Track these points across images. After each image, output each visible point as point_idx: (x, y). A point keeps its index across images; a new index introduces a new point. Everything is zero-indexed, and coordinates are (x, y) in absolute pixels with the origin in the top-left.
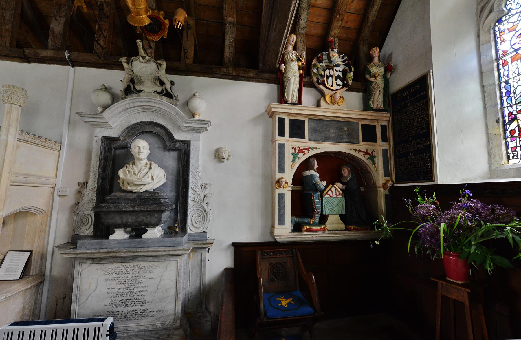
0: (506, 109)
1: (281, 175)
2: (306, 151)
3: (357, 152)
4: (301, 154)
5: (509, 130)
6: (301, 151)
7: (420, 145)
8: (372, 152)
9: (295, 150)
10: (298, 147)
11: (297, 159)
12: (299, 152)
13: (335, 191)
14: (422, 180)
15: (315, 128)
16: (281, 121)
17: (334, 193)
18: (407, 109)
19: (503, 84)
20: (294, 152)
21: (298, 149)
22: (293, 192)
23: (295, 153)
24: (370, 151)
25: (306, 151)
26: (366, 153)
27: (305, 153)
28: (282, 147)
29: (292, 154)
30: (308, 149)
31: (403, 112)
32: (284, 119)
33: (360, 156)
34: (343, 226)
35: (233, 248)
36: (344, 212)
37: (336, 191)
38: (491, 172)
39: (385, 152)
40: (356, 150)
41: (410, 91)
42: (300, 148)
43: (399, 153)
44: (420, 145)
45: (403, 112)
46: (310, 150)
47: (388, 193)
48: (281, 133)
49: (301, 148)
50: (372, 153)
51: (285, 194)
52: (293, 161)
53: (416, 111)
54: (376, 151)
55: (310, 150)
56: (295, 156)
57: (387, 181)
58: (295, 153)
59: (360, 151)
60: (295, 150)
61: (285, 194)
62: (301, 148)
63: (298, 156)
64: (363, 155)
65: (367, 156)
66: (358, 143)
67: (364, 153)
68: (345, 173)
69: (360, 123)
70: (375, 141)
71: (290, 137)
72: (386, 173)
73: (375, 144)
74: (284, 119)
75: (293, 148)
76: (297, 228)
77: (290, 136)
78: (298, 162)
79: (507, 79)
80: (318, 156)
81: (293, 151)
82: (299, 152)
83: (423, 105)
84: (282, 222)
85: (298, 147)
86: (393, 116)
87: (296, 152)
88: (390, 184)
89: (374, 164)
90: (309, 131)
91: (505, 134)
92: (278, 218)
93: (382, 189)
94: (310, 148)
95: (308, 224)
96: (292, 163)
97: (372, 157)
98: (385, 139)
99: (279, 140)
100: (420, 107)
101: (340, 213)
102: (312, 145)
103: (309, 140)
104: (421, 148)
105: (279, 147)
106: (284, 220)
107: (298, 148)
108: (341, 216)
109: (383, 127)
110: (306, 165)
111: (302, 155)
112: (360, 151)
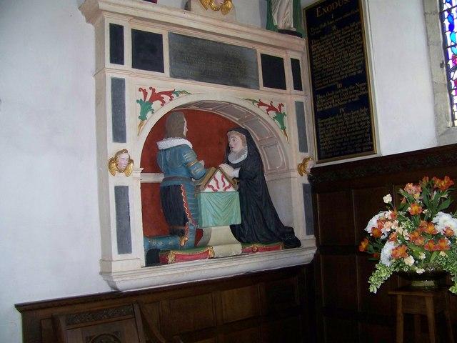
0: (449, 49)
1: (120, 146)
2: (166, 98)
3: (256, 104)
4: (157, 104)
5: (454, 79)
6: (157, 96)
7: (353, 96)
8: (280, 108)
9: (145, 94)
10: (151, 88)
11: (150, 113)
12: (153, 99)
13: (222, 179)
14: (359, 152)
15: (182, 52)
16: (116, 32)
17: (221, 184)
18: (331, 35)
19: (446, 14)
20: (142, 97)
21: (150, 93)
22: (144, 186)
23: (145, 98)
24: (276, 105)
25: (166, 98)
26: (271, 108)
27: (163, 103)
28: (118, 85)
29: (138, 101)
30: (169, 93)
31: (326, 39)
32: (121, 28)
33: (261, 111)
34: (238, 247)
35: (18, 317)
36: (238, 220)
37: (224, 179)
38: (439, 135)
39: (299, 106)
40: (254, 101)
41: (335, 5)
42: (154, 90)
43: (321, 109)
44: (353, 96)
45: (326, 39)
46: (174, 95)
47: (307, 182)
48: (117, 57)
49: (157, 92)
50: (281, 105)
51: (128, 187)
52: (143, 118)
53: (345, 39)
54: (285, 104)
55: (174, 95)
56: (146, 107)
57: (306, 160)
58: (145, 98)
59: (261, 104)
60: (145, 94)
61: (128, 187)
62: (157, 92)
63: (150, 108)
64: (266, 111)
65: (273, 114)
66: (257, 88)
67: (267, 108)
68: (235, 145)
69: (261, 50)
70: (282, 86)
71: (134, 66)
72: (303, 148)
73: (284, 91)
74: (121, 28)
75: (140, 90)
76: (154, 258)
77: (134, 66)
78: (152, 120)
79: (450, 6)
80: (186, 111)
81: (141, 96)
82: (153, 99)
83: (355, 31)
84: (124, 246)
85: (151, 88)
86: (310, 44)
87: (148, 99)
88: (310, 165)
89: (284, 128)
90: (170, 58)
91: (449, 84)
92: (118, 238)
93: (296, 174)
94: (173, 92)
95: (176, 247)
96: (140, 120)
97: (280, 117)
98: (298, 86)
99: (114, 71)
100: (350, 33)
101: (232, 223)
102: (179, 84)
103: (171, 76)
104: (355, 100)
105: (112, 86)
106: (130, 242)
107: (151, 91)
108: (233, 227)
109: (295, 63)
110: (161, 131)
111: (160, 106)
112: (261, 104)
